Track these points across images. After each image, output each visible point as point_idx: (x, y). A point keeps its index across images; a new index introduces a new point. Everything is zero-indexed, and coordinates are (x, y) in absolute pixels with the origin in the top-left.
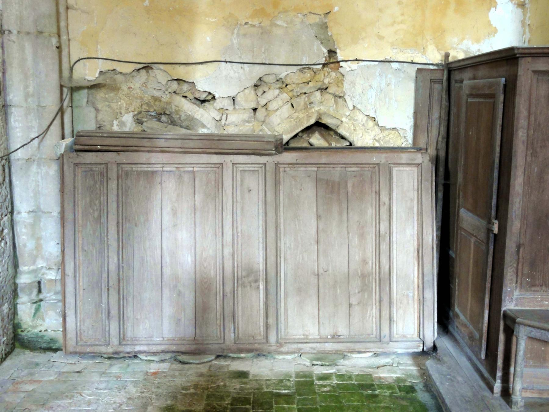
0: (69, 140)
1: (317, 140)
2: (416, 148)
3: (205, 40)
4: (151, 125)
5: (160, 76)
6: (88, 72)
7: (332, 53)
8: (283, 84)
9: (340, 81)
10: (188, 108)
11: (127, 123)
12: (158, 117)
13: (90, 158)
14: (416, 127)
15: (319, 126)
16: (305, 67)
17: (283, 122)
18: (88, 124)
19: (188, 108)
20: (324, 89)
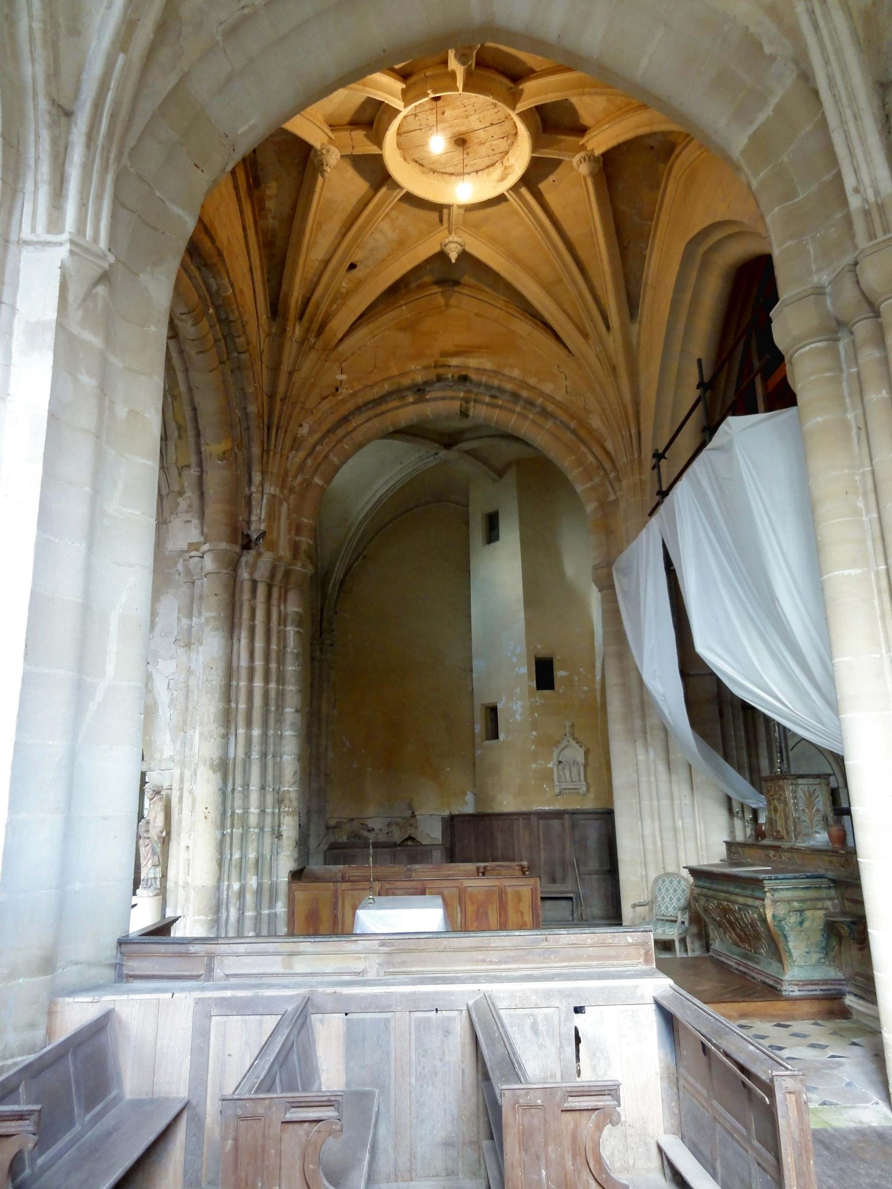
0: (327, 846)
1: (409, 843)
2: (443, 844)
3: (371, 810)
4: (353, 840)
5: (356, 823)
6: (332, 822)
7: (413, 813)
8: (397, 824)
9: (417, 821)
10: (365, 833)
11: (344, 839)
12: (355, 837)
13: (336, 851)
14: (443, 837)
15: (410, 838)
16: (404, 818)
17: (398, 837)
18: (332, 840)
19: (365, 833)
20: (411, 825)
